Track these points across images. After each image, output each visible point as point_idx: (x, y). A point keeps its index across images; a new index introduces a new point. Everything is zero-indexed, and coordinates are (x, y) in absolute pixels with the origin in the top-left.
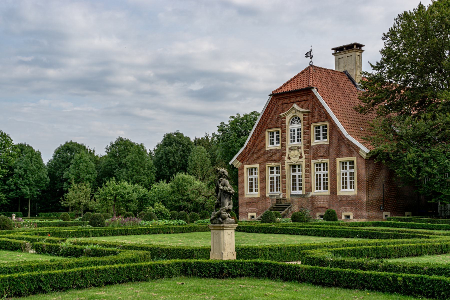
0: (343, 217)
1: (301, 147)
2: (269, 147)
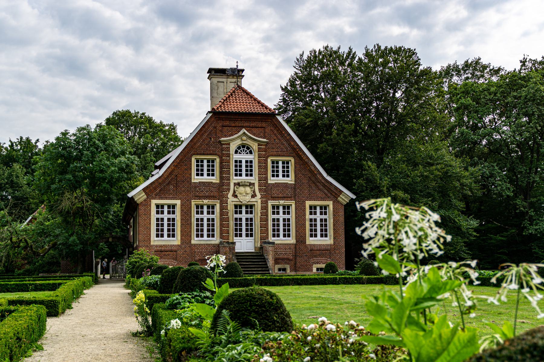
0: (315, 270)
1: (254, 183)
2: (196, 179)
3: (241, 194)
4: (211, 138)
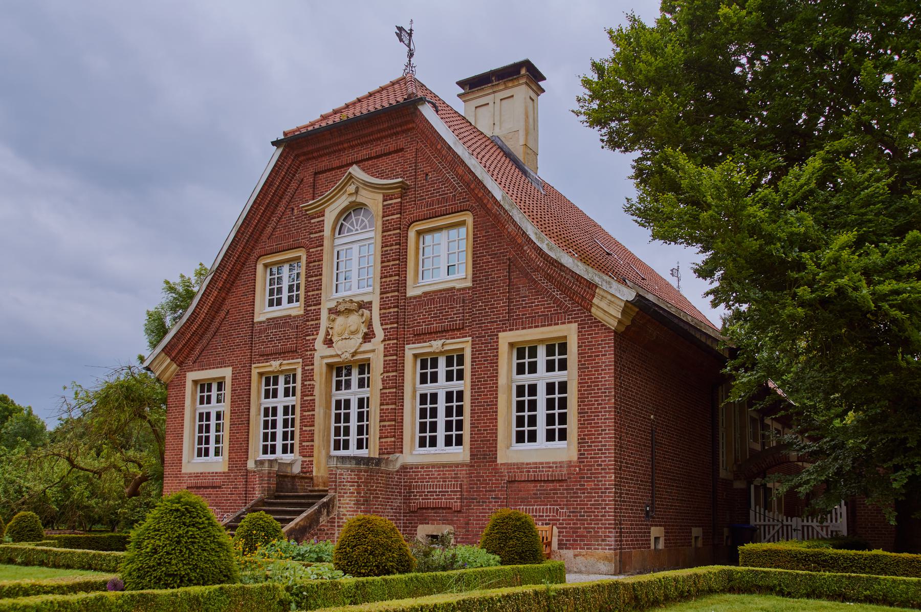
1: (370, 303)
2: (263, 312)
3: (340, 335)
4: (293, 209)
